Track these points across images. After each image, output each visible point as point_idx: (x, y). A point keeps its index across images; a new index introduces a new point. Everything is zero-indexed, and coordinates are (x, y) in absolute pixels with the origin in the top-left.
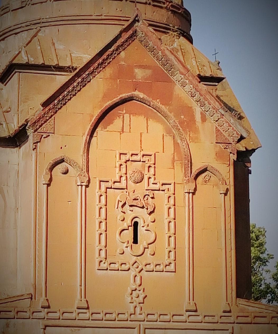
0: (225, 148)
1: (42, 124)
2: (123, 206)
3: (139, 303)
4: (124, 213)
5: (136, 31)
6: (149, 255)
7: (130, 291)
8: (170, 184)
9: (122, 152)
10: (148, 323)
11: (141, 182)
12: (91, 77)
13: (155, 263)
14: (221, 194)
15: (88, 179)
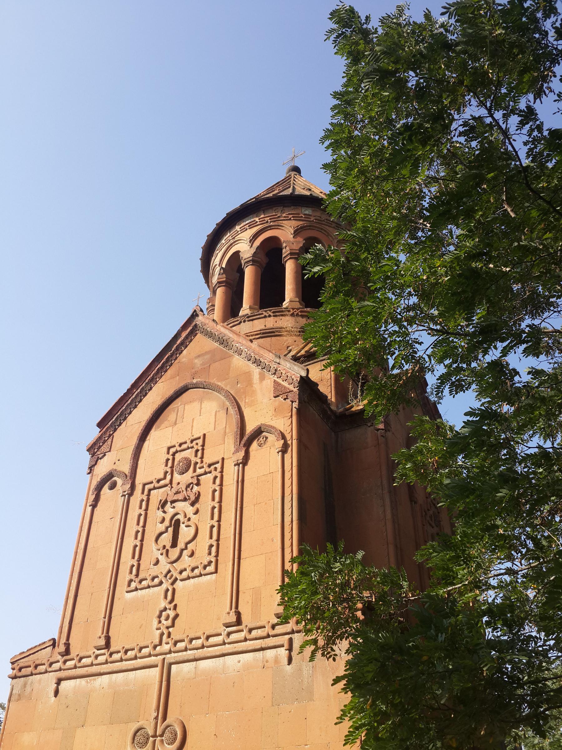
0: (285, 399)
1: (100, 447)
2: (163, 505)
3: (168, 628)
4: (164, 512)
5: (196, 326)
6: (187, 557)
7: (158, 613)
8: (218, 462)
9: (169, 445)
10: (176, 654)
11: (187, 471)
12: (152, 385)
13: (193, 565)
14: (278, 452)
15: (129, 486)
